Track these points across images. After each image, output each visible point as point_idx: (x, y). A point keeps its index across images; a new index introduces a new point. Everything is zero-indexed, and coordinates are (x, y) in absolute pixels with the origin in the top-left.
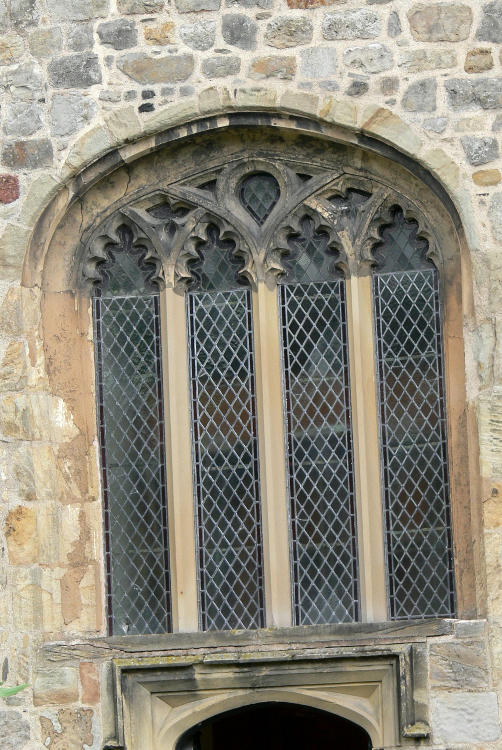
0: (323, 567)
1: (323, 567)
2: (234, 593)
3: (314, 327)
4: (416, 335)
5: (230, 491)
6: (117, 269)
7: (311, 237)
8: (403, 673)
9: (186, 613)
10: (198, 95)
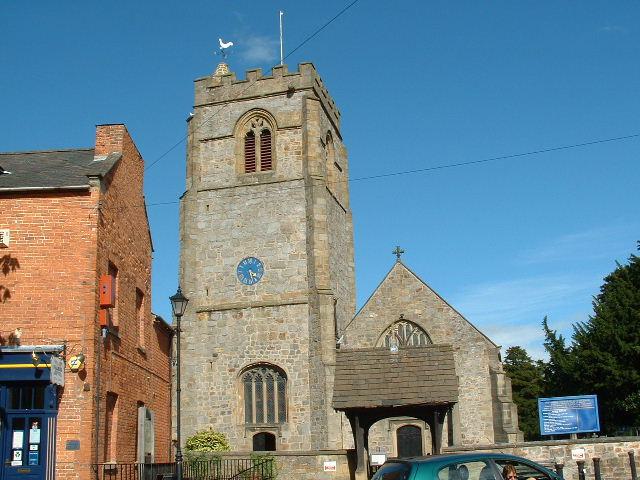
0: (271, 417)
1: (271, 417)
2: (260, 418)
3: (271, 389)
4: (282, 388)
5: (260, 406)
6: (248, 379)
7: (270, 378)
8: (279, 429)
9: (254, 421)
10: (257, 360)
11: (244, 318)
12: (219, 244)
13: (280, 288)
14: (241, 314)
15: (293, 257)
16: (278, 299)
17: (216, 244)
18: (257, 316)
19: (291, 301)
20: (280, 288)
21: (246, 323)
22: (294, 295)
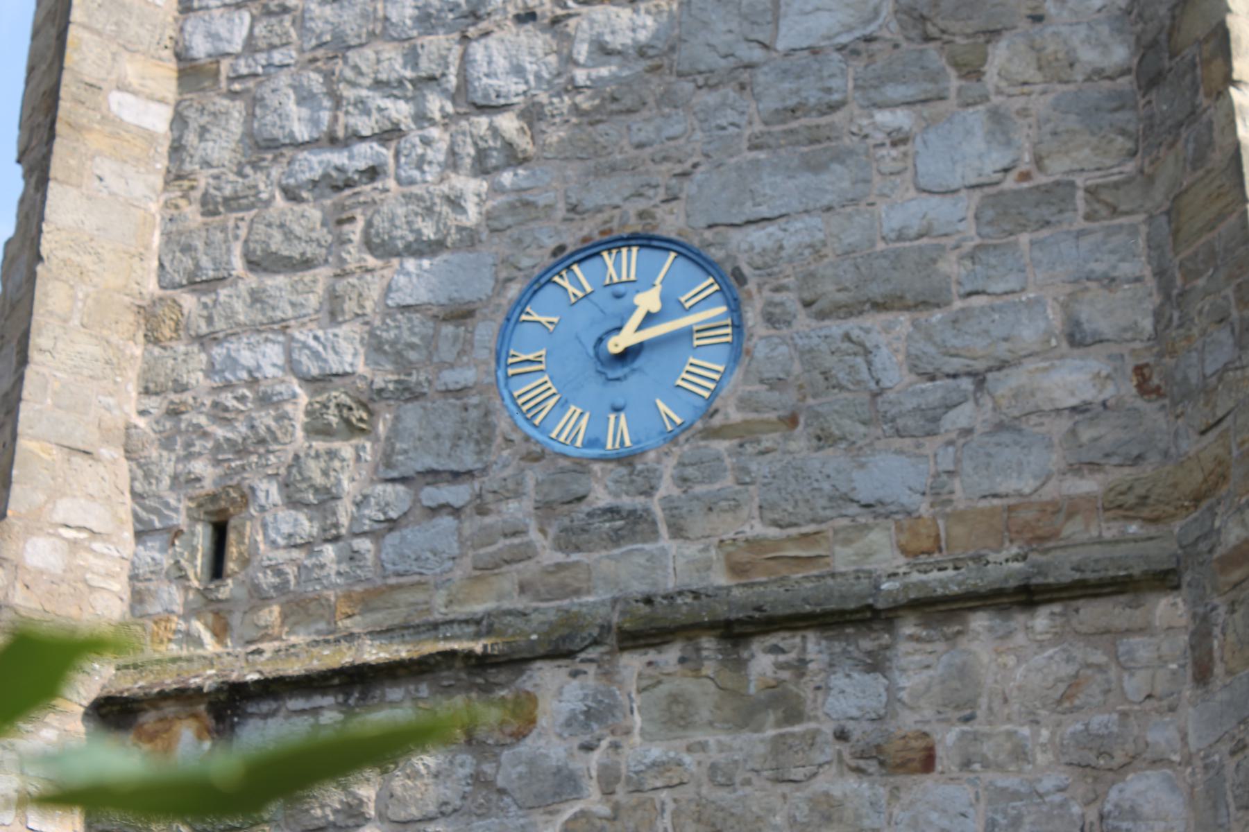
11: (549, 745)
12: (364, 155)
13: (892, 474)
14: (523, 719)
15: (1014, 207)
16: (876, 559)
17: (314, 164)
18: (676, 716)
19: (1005, 565)
20: (892, 474)
21: (565, 784)
22: (1035, 524)
